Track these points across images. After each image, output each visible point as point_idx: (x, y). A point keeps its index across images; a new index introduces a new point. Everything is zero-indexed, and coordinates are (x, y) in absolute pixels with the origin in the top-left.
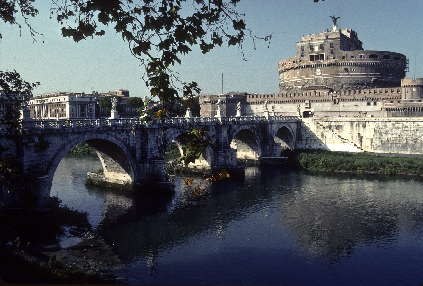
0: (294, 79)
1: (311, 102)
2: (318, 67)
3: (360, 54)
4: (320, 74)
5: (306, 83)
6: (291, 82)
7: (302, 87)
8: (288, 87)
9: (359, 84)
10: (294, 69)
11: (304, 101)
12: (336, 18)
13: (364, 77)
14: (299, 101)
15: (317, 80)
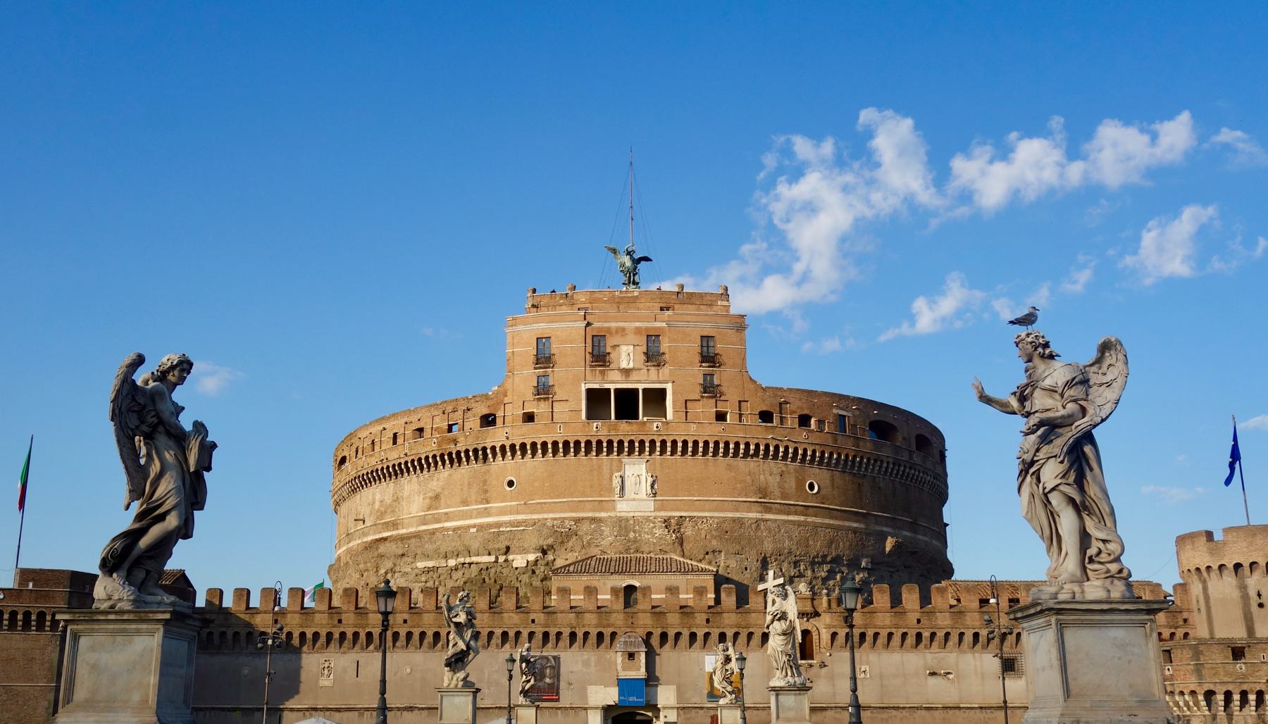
0: (487, 512)
1: (655, 641)
2: (631, 452)
3: (835, 411)
4: (645, 488)
5: (564, 536)
6: (455, 529)
7: (537, 561)
8: (427, 557)
9: (836, 560)
10: (481, 454)
11: (607, 639)
12: (636, 256)
13: (855, 525)
14: (580, 635)
15: (623, 525)
